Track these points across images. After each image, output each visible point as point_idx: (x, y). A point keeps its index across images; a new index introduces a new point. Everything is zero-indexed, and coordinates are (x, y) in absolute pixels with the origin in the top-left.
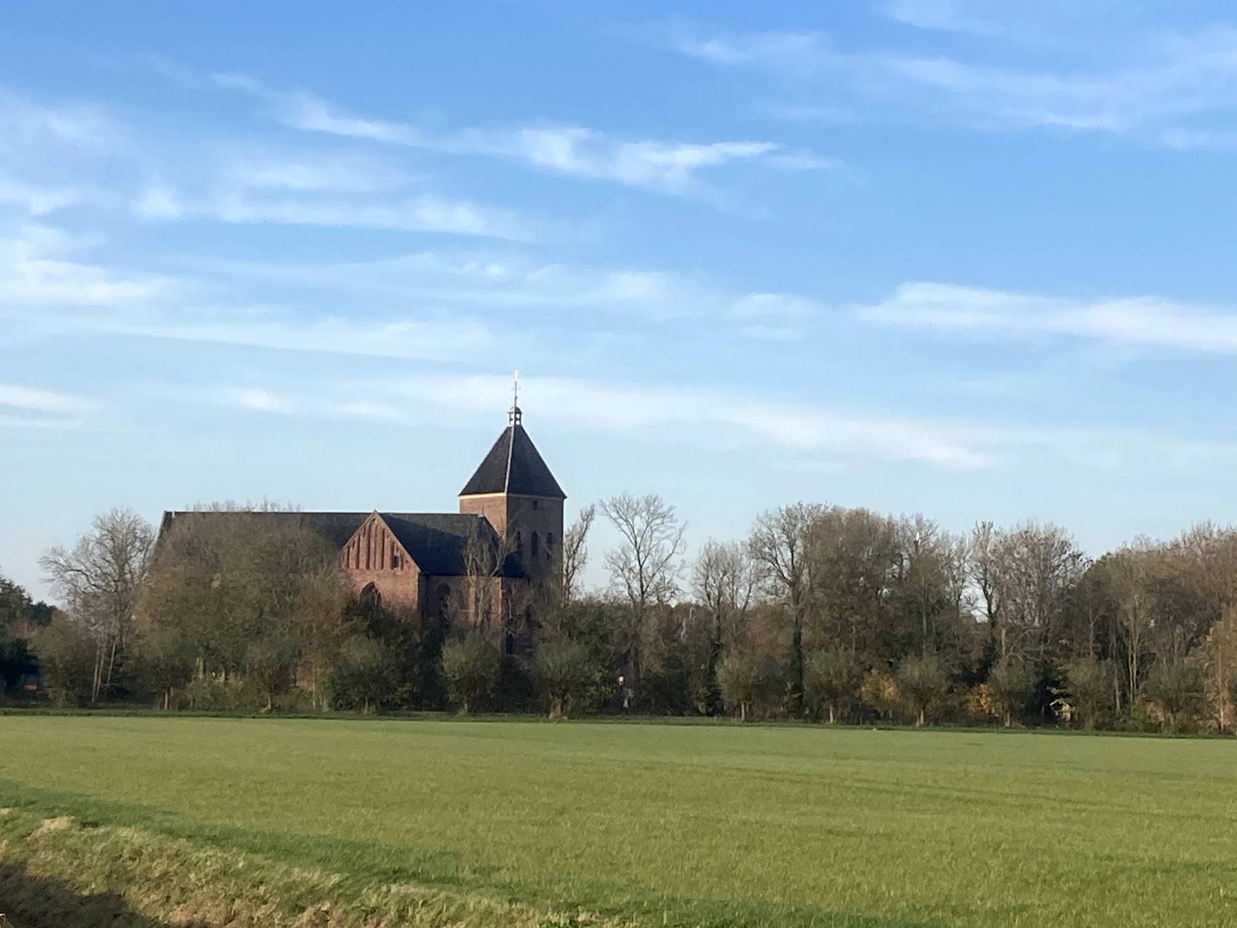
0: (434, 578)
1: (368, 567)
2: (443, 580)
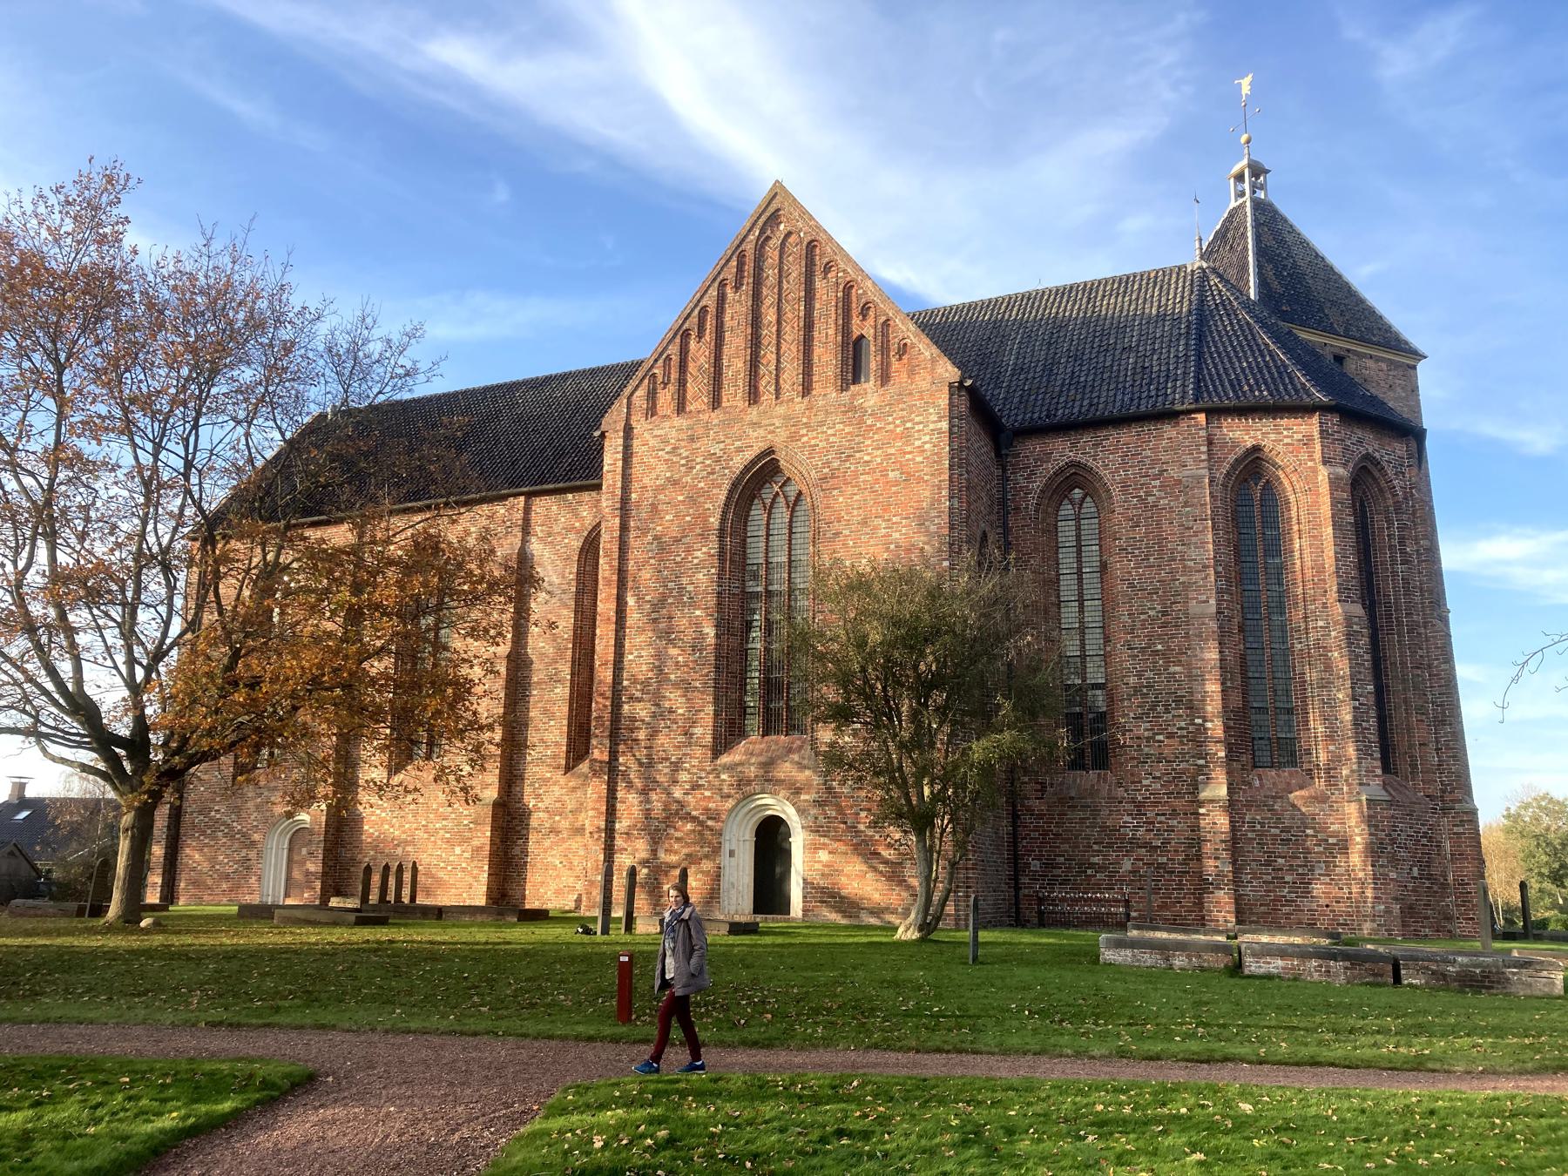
1: (753, 396)
2: (1062, 451)
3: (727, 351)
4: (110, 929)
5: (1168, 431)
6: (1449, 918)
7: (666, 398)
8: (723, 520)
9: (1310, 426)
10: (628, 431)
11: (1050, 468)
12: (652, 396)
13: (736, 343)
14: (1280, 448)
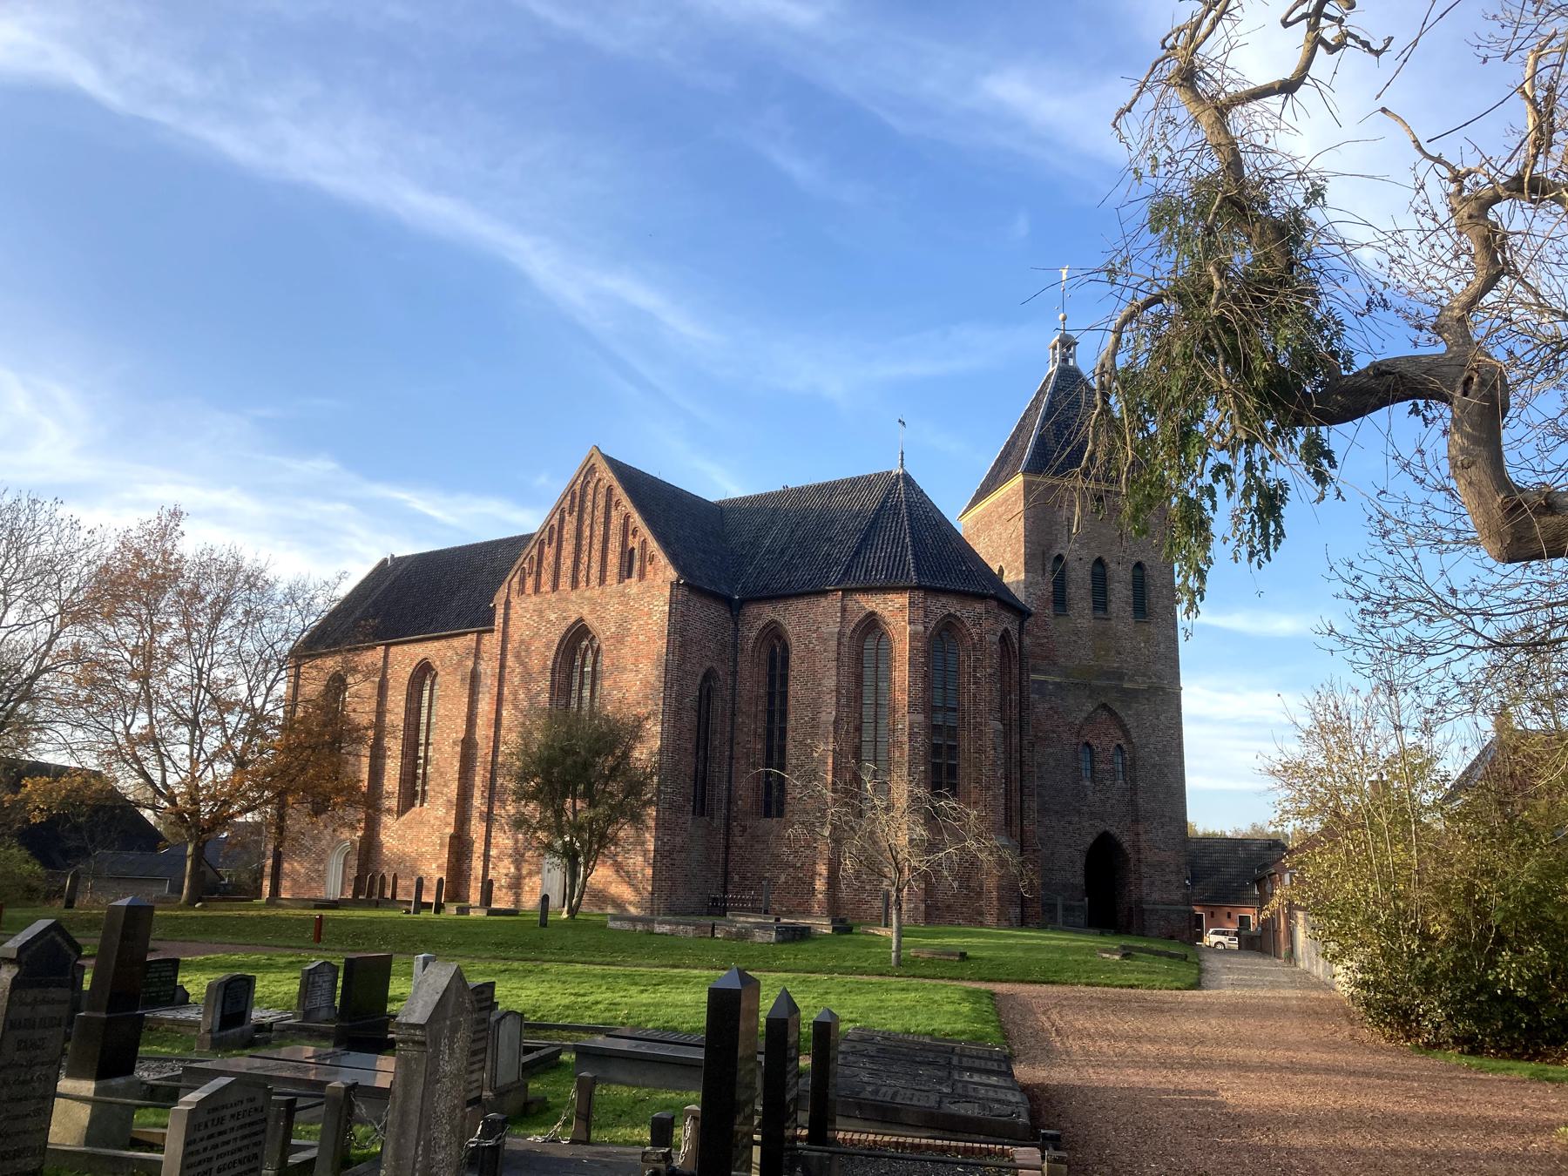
0: (752, 610)
1: (575, 584)
2: (768, 612)
3: (564, 553)
4: (180, 908)
5: (824, 602)
6: (981, 914)
7: (530, 582)
8: (555, 662)
9: (902, 600)
10: (508, 604)
11: (761, 624)
12: (522, 581)
13: (568, 548)
14: (886, 613)
